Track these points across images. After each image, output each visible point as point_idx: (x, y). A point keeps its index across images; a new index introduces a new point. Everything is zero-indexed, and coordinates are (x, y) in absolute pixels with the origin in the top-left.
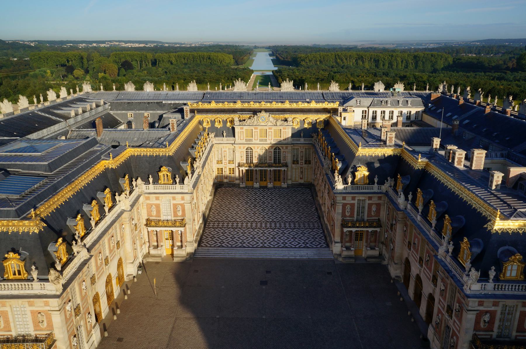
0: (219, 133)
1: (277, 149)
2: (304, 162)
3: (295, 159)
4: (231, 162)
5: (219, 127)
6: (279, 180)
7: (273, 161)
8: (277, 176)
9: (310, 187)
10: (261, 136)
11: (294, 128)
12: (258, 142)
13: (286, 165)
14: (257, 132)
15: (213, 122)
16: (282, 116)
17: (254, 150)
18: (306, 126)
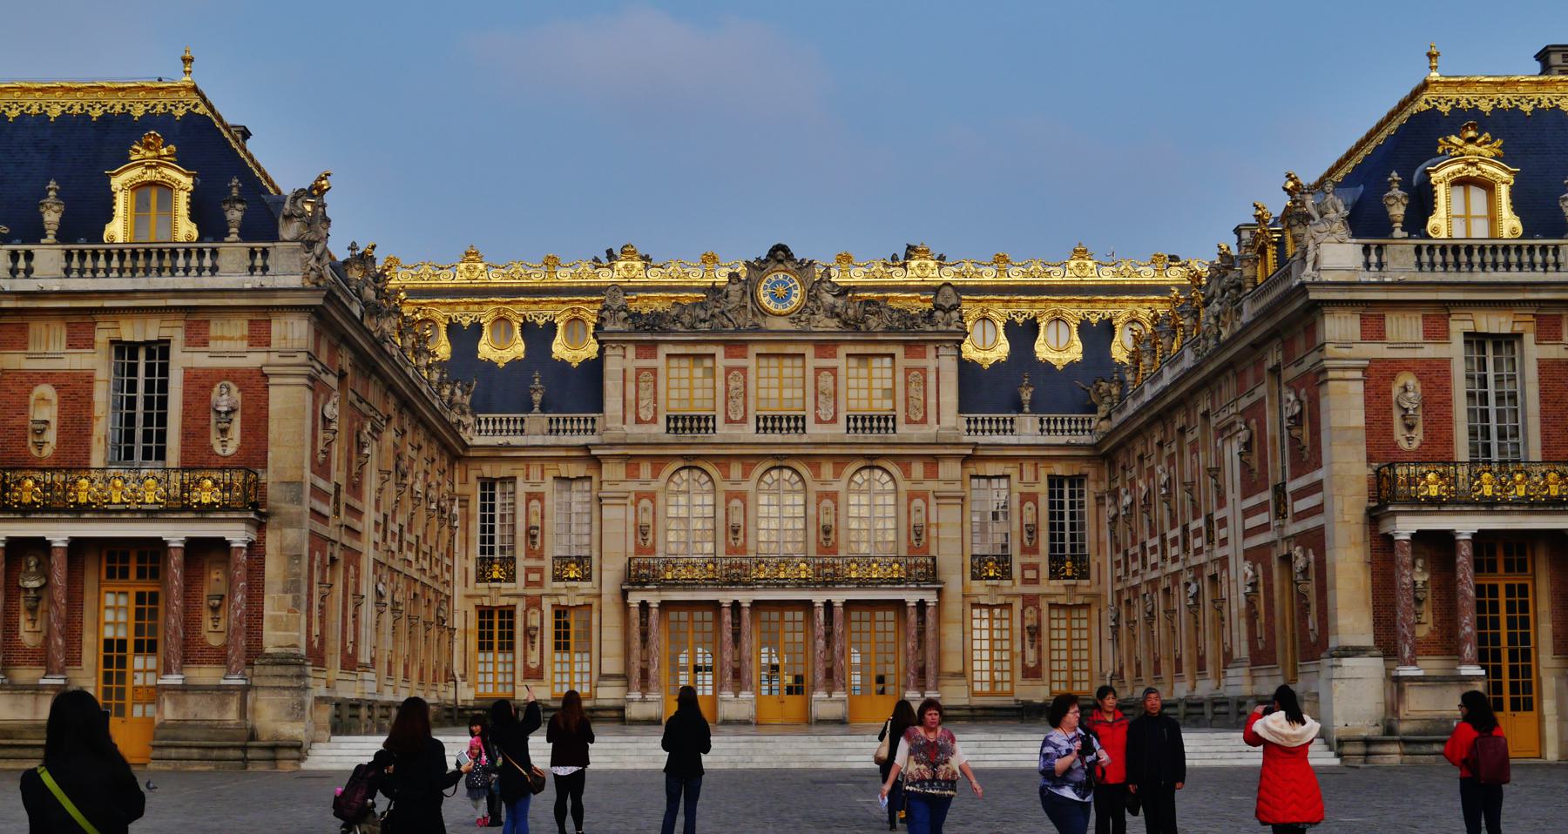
2: (1042, 559)
11: (974, 365)
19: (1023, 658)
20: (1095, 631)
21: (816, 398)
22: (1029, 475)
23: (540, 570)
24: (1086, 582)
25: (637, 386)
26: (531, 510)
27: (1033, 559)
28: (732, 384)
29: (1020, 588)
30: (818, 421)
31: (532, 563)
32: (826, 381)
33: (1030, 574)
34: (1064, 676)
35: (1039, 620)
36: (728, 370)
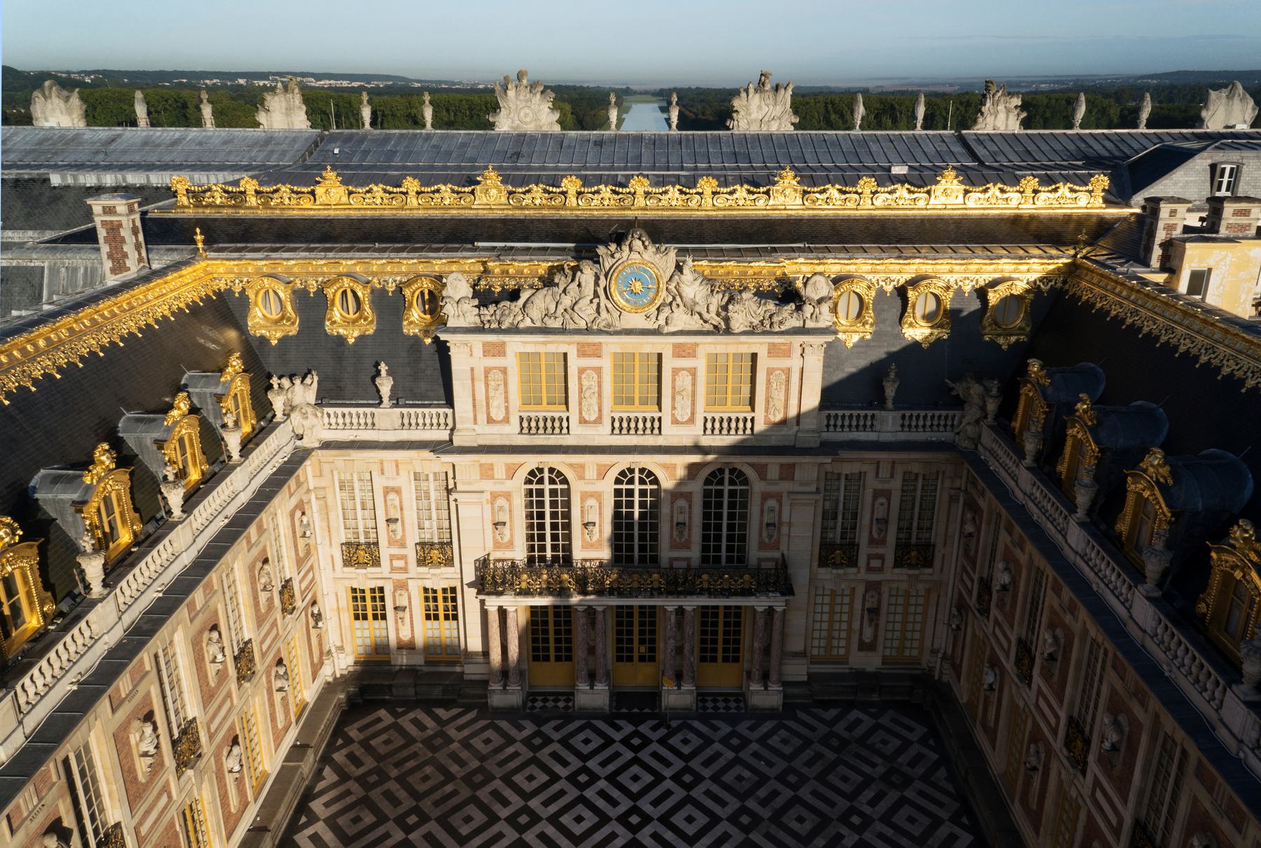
0: (344, 379)
1: (725, 481)
2: (889, 551)
3: (835, 536)
4: (435, 552)
5: (352, 335)
6: (733, 656)
7: (695, 553)
8: (720, 637)
9: (918, 698)
10: (623, 399)
12: (602, 435)
13: (778, 579)
14: (597, 373)
15: (312, 306)
16: (764, 269)
17: (577, 488)
18: (917, 331)
19: (861, 634)
20: (932, 612)
21: (673, 399)
22: (884, 472)
23: (404, 557)
24: (929, 571)
25: (487, 385)
26: (389, 503)
27: (880, 551)
28: (585, 383)
29: (863, 575)
30: (675, 422)
31: (396, 551)
32: (684, 381)
33: (876, 563)
34: (896, 643)
35: (879, 602)
36: (581, 371)
